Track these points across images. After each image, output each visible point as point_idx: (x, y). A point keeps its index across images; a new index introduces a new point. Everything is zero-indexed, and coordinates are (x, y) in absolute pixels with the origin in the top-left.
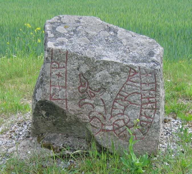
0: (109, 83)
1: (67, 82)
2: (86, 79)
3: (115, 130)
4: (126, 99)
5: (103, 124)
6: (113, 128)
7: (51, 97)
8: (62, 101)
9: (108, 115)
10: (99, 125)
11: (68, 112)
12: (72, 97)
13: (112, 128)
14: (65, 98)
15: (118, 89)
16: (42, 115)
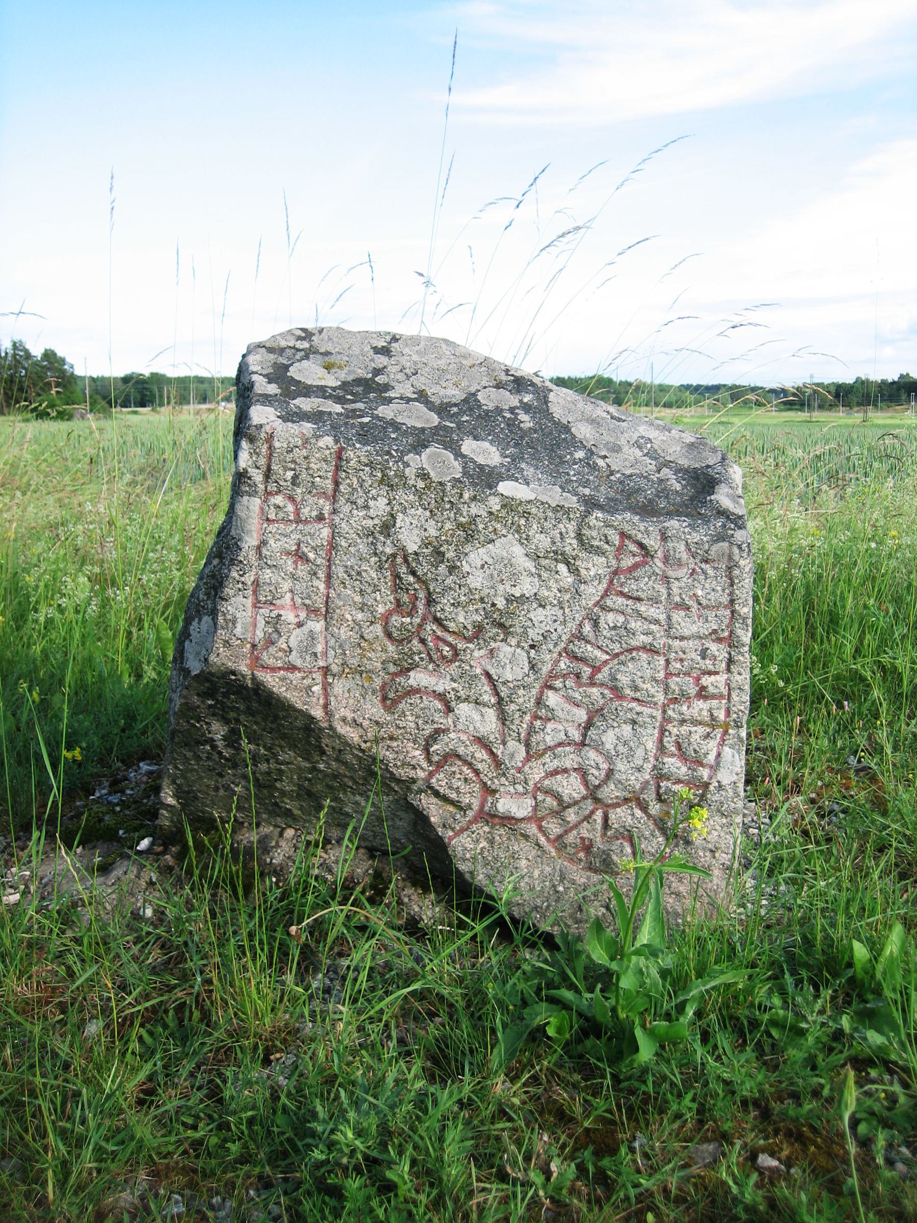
0: (522, 599)
1: (332, 591)
2: (419, 579)
3: (542, 819)
4: (599, 676)
5: (489, 791)
6: (535, 808)
7: (256, 661)
8: (303, 678)
9: (512, 744)
10: (471, 797)
11: (331, 728)
12: (354, 662)
13: (530, 809)
14: (321, 663)
15: (565, 632)
16: (212, 740)
